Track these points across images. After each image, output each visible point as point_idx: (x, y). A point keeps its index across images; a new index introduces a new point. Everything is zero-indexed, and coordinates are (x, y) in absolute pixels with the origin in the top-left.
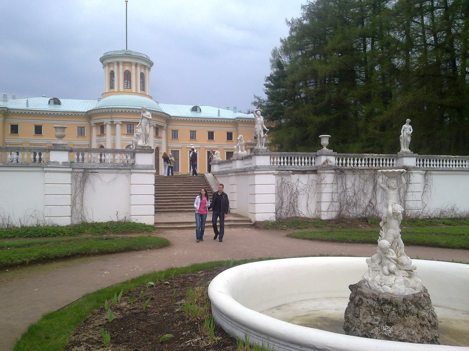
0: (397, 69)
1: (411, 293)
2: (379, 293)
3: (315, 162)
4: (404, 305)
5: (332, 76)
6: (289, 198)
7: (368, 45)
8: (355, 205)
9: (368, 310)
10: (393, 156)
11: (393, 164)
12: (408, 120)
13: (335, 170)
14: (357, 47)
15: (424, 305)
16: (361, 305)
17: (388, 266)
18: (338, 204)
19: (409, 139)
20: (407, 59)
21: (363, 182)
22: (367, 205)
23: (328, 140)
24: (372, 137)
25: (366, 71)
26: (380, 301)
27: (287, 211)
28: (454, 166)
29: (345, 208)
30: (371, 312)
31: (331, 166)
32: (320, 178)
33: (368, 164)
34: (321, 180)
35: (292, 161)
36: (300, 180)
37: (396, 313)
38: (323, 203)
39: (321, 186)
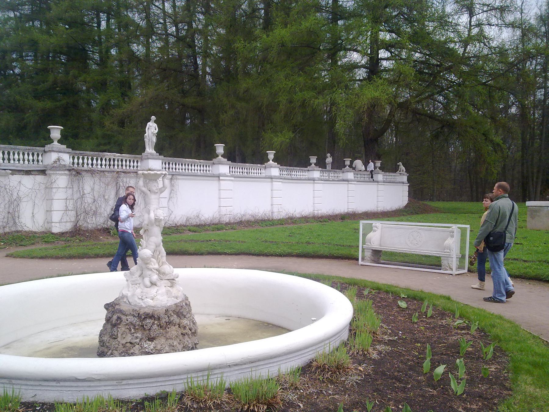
0: (137, 57)
1: (173, 303)
2: (140, 307)
3: (42, 160)
4: (166, 316)
5: (58, 52)
6: (7, 206)
7: (102, 22)
8: (95, 213)
9: (128, 329)
10: (138, 158)
11: (137, 167)
12: (153, 118)
13: (69, 170)
14: (89, 22)
15: (185, 314)
16: (119, 324)
17: (150, 278)
18: (73, 213)
19: (154, 139)
20: (147, 46)
21: (104, 186)
22: (108, 213)
23: (59, 132)
24: (109, 133)
25: (100, 52)
26: (141, 317)
27: (5, 224)
28: (199, 171)
29: (82, 218)
30: (130, 330)
31: (65, 166)
32: (50, 181)
33: (110, 165)
34: (52, 183)
35: (10, 157)
36: (23, 182)
37: (158, 326)
38: (55, 212)
39: (51, 191)
